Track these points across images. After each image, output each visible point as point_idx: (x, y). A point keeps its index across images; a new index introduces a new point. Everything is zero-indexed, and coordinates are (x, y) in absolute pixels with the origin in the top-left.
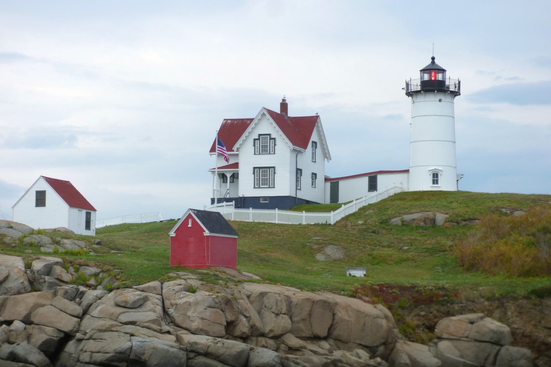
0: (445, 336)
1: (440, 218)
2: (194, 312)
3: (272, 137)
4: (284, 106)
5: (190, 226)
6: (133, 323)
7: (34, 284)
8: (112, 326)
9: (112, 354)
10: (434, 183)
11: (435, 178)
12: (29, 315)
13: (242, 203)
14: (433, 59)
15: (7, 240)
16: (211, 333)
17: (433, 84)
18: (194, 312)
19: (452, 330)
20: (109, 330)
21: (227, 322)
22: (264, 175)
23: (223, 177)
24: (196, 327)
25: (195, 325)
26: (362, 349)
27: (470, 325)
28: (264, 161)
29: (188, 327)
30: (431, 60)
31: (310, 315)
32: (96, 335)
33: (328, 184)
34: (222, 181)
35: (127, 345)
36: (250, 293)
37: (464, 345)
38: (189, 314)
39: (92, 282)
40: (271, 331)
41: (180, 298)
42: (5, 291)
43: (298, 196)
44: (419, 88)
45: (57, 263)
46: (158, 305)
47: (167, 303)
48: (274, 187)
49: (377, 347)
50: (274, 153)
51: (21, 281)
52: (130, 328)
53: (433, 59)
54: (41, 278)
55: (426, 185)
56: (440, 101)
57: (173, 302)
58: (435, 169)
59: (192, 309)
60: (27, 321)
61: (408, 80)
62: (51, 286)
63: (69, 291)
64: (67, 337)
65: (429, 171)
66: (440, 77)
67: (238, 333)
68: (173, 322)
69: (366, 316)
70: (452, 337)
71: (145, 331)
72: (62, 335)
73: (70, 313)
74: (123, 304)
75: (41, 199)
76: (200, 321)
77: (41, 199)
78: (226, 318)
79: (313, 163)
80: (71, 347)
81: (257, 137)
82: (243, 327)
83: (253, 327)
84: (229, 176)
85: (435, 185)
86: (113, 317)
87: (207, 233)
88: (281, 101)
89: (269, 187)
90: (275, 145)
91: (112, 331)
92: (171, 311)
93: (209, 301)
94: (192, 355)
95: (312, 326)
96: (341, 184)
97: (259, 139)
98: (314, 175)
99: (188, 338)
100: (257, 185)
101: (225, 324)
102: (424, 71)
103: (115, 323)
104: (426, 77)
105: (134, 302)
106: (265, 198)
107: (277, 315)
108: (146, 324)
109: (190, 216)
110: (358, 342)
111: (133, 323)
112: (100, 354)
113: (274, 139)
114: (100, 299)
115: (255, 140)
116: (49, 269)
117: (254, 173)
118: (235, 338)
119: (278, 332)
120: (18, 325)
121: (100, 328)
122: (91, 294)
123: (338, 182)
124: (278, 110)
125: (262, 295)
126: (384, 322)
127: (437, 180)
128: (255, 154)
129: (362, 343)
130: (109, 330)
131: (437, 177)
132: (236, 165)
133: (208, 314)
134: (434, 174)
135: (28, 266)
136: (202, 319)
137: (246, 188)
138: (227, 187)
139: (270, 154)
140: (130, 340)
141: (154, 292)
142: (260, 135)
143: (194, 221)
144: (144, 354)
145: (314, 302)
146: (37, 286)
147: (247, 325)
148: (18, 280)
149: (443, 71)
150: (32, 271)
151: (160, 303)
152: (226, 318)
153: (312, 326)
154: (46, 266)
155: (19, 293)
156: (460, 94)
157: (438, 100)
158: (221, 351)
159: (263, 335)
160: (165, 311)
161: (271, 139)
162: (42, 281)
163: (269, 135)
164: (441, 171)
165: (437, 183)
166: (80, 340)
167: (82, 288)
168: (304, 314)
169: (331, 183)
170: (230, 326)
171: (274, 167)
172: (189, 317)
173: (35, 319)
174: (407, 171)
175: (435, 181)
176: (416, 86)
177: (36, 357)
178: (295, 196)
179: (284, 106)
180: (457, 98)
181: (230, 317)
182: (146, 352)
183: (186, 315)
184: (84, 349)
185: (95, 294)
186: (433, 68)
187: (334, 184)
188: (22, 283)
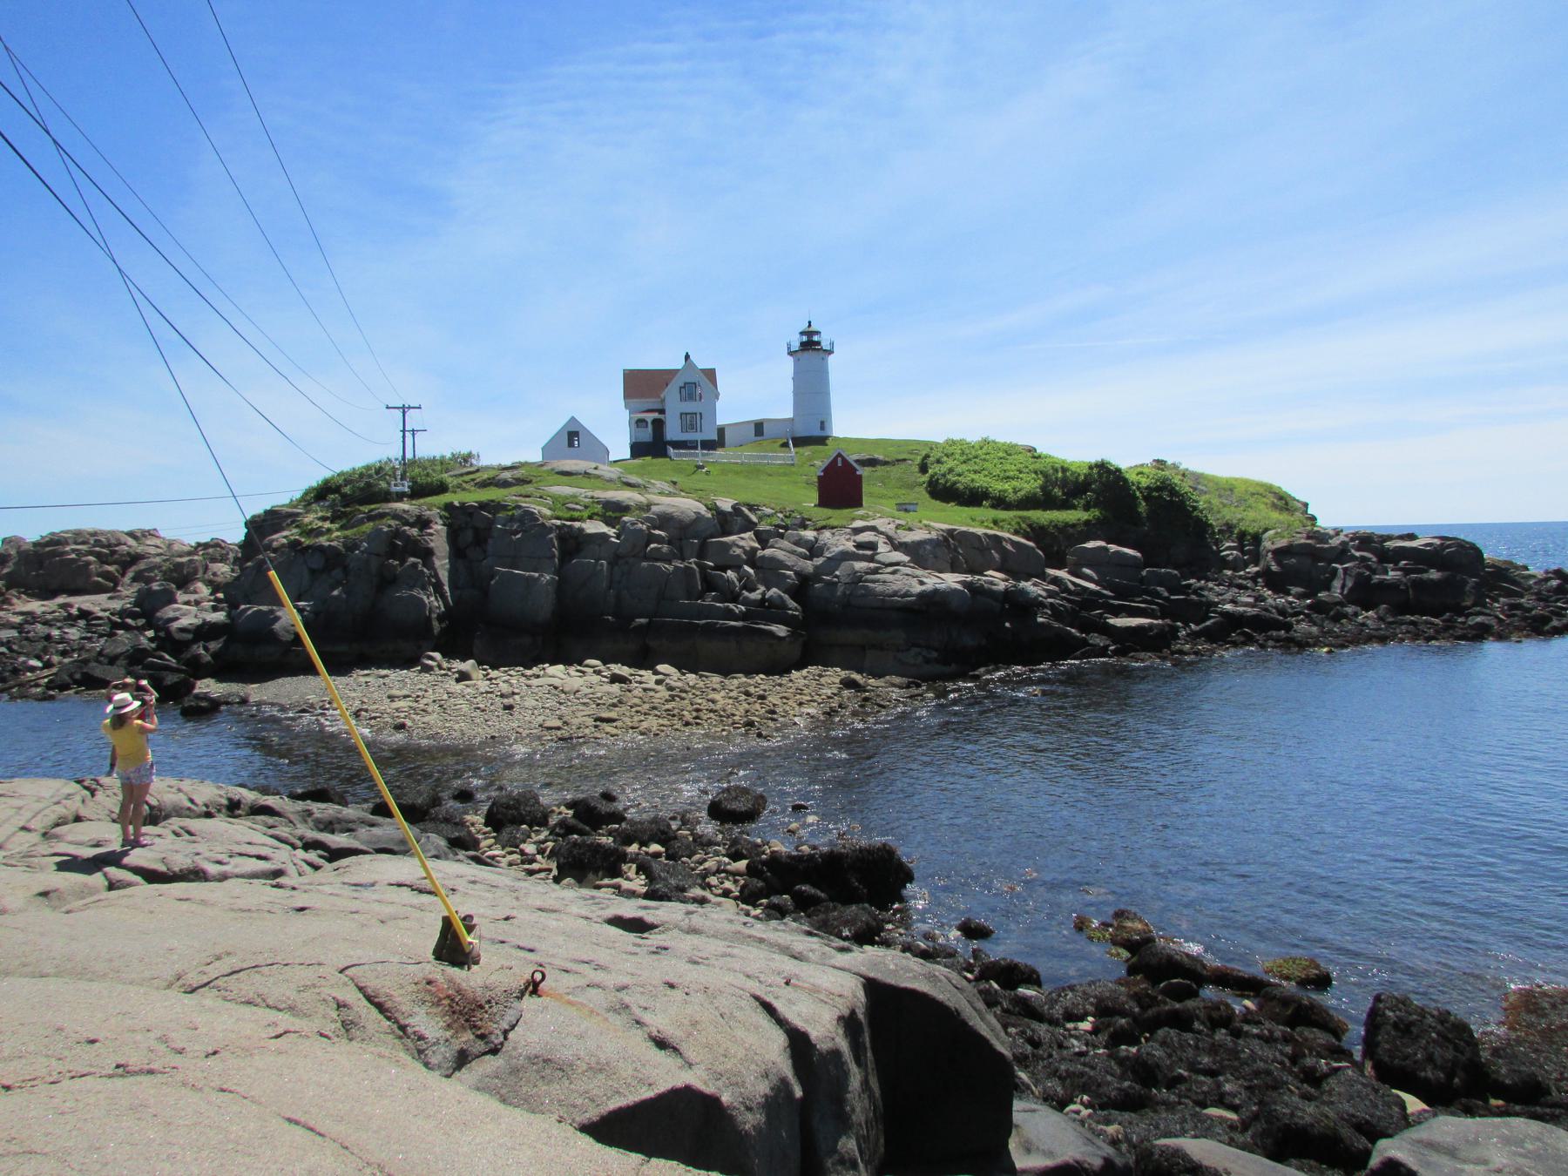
6: (897, 564)
11: (823, 425)
17: (810, 344)
20: (875, 571)
28: (690, 407)
104: (805, 338)
109: (839, 455)
130: (875, 571)
132: (662, 411)
140: (922, 583)
143: (845, 461)
176: (796, 346)
186: (809, 333)
187: (721, 431)
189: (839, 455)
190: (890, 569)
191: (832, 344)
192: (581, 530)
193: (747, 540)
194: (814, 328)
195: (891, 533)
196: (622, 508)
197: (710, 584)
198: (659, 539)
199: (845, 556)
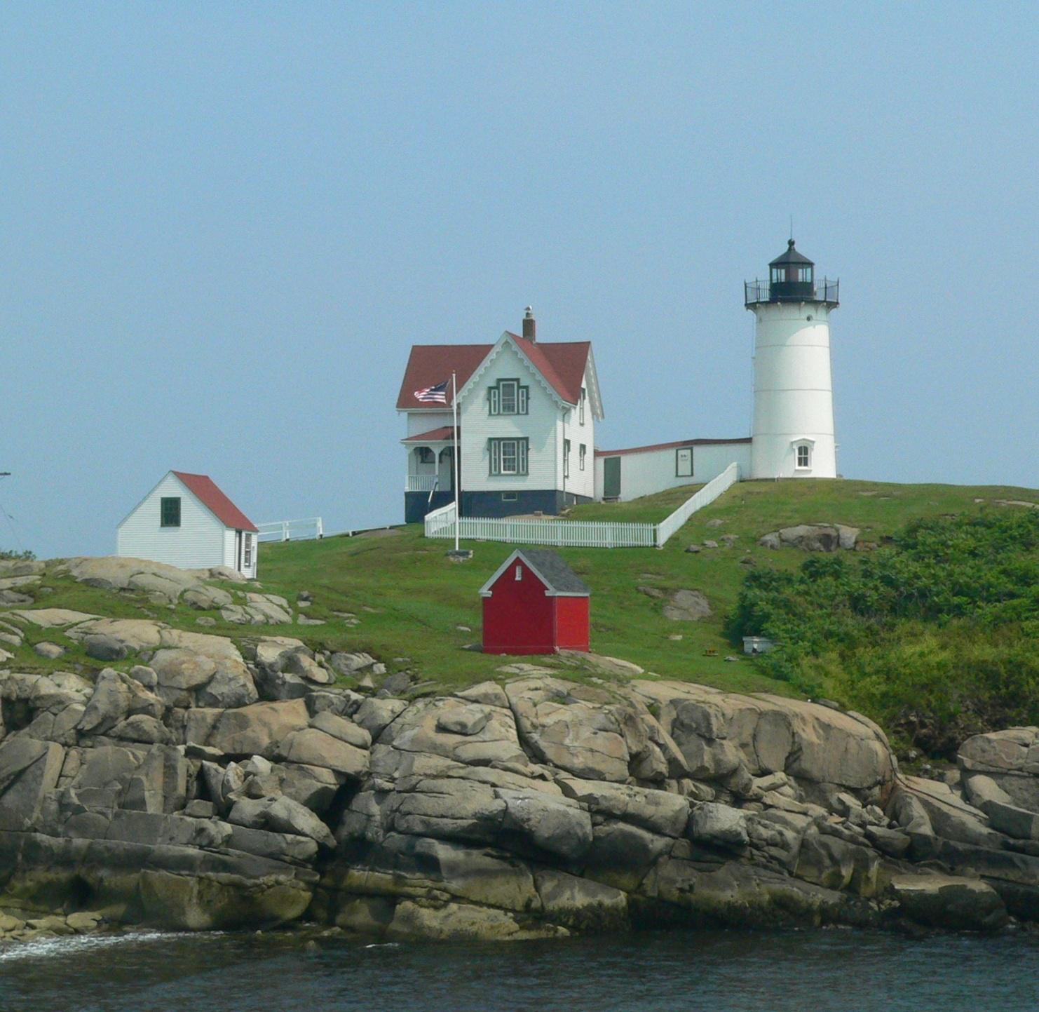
0: (980, 767)
1: (849, 534)
2: (576, 738)
3: (522, 384)
4: (529, 325)
5: (518, 578)
6: (485, 763)
8: (449, 768)
9: (470, 821)
10: (800, 464)
11: (804, 454)
12: (276, 744)
13: (474, 504)
14: (791, 243)
16: (608, 776)
18: (576, 738)
21: (631, 755)
22: (509, 452)
23: (423, 454)
24: (581, 766)
25: (578, 762)
26: (846, 792)
27: (1025, 749)
28: (507, 427)
29: (569, 766)
30: (788, 246)
31: (754, 737)
32: (427, 784)
33: (601, 461)
34: (420, 459)
35: (498, 805)
36: (653, 702)
37: (1016, 783)
38: (567, 741)
39: (367, 682)
41: (548, 714)
42: (211, 701)
43: (567, 490)
44: (765, 296)
45: (297, 649)
46: (510, 727)
47: (526, 724)
48: (527, 474)
49: (869, 788)
50: (527, 413)
51: (242, 682)
52: (482, 771)
53: (791, 243)
54: (278, 678)
55: (789, 468)
56: (809, 319)
57: (535, 720)
58: (804, 439)
59: (571, 735)
61: (750, 280)
63: (335, 701)
64: (351, 784)
65: (792, 443)
66: (802, 275)
67: (646, 771)
68: (536, 755)
69: (849, 736)
70: (992, 769)
71: (509, 777)
72: (343, 781)
73: (351, 740)
74: (458, 728)
75: (171, 513)
76: (589, 754)
77: (171, 513)
78: (629, 748)
79: (581, 428)
81: (493, 384)
83: (672, 762)
84: (437, 452)
85: (803, 468)
88: (524, 317)
89: (518, 474)
90: (528, 398)
91: (449, 777)
92: (535, 736)
93: (600, 719)
94: (599, 818)
95: (758, 756)
97: (497, 388)
98: (583, 447)
99: (582, 787)
100: (494, 473)
101: (628, 758)
102: (774, 265)
104: (781, 275)
105: (475, 724)
106: (510, 494)
108: (510, 765)
109: (518, 562)
110: (836, 782)
111: (485, 763)
112: (445, 820)
113: (526, 387)
114: (398, 716)
115: (490, 388)
116: (291, 663)
117: (489, 450)
118: (645, 782)
120: (261, 764)
121: (428, 772)
122: (386, 707)
123: (619, 458)
124: (519, 332)
126: (877, 746)
127: (806, 459)
128: (490, 414)
129: (844, 782)
131: (806, 453)
133: (601, 741)
134: (800, 449)
135: (249, 655)
136: (592, 750)
137: (476, 475)
138: (434, 473)
139: (518, 413)
140: (497, 796)
141: (497, 703)
142: (499, 380)
143: (526, 571)
144: (529, 820)
145: (761, 715)
147: (663, 759)
149: (811, 264)
150: (258, 665)
151: (513, 724)
152: (629, 748)
153: (758, 756)
154: (281, 655)
157: (804, 316)
159: (687, 775)
160: (524, 740)
161: (519, 387)
162: (279, 682)
163: (517, 380)
164: (813, 442)
165: (806, 464)
166: (382, 794)
167: (355, 696)
168: (746, 737)
169: (606, 461)
170: (636, 761)
171: (526, 439)
172: (568, 748)
174: (748, 441)
177: (308, 821)
178: (562, 489)
179: (529, 325)
180: (834, 310)
181: (635, 749)
182: (532, 816)
183: (562, 744)
184: (404, 808)
185: (390, 708)
188: (244, 685)
192: (35, 686)
193: (290, 713)
194: (801, 249)
195: (522, 707)
196: (112, 654)
197: (203, 786)
198: (147, 709)
199: (421, 747)
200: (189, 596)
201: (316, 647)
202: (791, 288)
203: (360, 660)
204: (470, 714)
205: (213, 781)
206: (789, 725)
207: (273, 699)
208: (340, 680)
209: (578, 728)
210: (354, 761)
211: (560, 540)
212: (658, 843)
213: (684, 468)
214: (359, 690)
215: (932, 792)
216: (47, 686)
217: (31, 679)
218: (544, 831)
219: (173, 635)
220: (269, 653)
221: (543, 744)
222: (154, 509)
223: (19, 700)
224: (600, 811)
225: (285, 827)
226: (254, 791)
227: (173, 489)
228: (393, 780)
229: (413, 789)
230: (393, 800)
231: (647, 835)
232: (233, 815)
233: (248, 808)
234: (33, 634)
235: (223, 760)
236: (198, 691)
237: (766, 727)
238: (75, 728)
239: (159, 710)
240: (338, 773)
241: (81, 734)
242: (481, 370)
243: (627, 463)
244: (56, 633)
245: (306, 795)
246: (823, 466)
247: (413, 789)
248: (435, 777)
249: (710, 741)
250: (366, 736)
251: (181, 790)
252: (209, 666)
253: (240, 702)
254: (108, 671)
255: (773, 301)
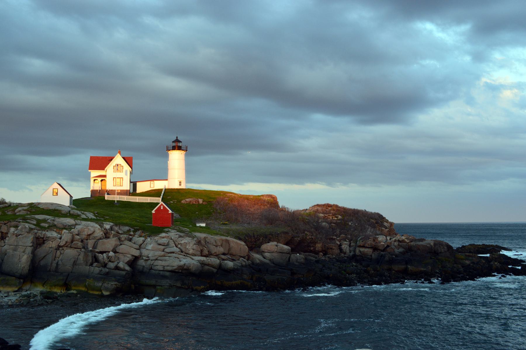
1: (201, 201)
5: (162, 208)
6: (173, 253)
7: (106, 235)
15: (63, 212)
19: (269, 249)
28: (119, 175)
32: (159, 258)
33: (132, 184)
38: (187, 247)
39: (132, 233)
40: (215, 253)
47: (177, 243)
60: (115, 252)
62: (114, 236)
64: (136, 259)
80: (141, 262)
82: (206, 252)
86: (159, 250)
87: (170, 212)
92: (179, 246)
93: (194, 242)
96: (138, 183)
102: (173, 142)
103: (163, 253)
104: (174, 144)
107: (216, 246)
109: (162, 204)
111: (173, 253)
119: (218, 254)
120: (111, 254)
125: (205, 238)
133: (195, 247)
143: (164, 207)
145: (223, 240)
146: (108, 235)
148: (99, 233)
149: (180, 142)
155: (100, 239)
156: (186, 151)
158: (214, 263)
159: (211, 254)
160: (176, 247)
167: (130, 237)
170: (202, 251)
173: (117, 251)
175: (180, 185)
177: (127, 268)
186: (177, 141)
189: (162, 204)
190: (169, 255)
191: (187, 147)
197: (96, 260)
200: (71, 212)
201: (116, 225)
202: (177, 146)
203: (127, 228)
204: (165, 241)
205: (100, 258)
206: (229, 243)
207: (109, 238)
208: (124, 233)
209: (189, 243)
210: (137, 253)
211: (137, 201)
212: (215, 270)
213: (152, 186)
214: (131, 235)
215: (257, 257)
216: (49, 234)
217: (44, 232)
218: (193, 269)
219: (78, 222)
220: (107, 226)
221: (181, 248)
222: (50, 190)
223: (41, 238)
224: (203, 264)
225: (124, 270)
226: (113, 260)
227: (56, 186)
228: (148, 257)
229: (156, 259)
230: (149, 262)
231: (213, 269)
232: (107, 266)
233: (112, 265)
234: (39, 222)
235: (102, 253)
236: (89, 235)
237: (224, 243)
238: (58, 245)
239: (80, 240)
240: (133, 256)
241: (59, 246)
242: (112, 162)
243: (138, 184)
244: (45, 221)
245: (126, 261)
246: (183, 186)
247: (156, 259)
248: (162, 256)
249: (216, 246)
250: (138, 247)
251: (91, 261)
252: (92, 229)
253: (100, 239)
254: (64, 231)
255: (173, 149)
